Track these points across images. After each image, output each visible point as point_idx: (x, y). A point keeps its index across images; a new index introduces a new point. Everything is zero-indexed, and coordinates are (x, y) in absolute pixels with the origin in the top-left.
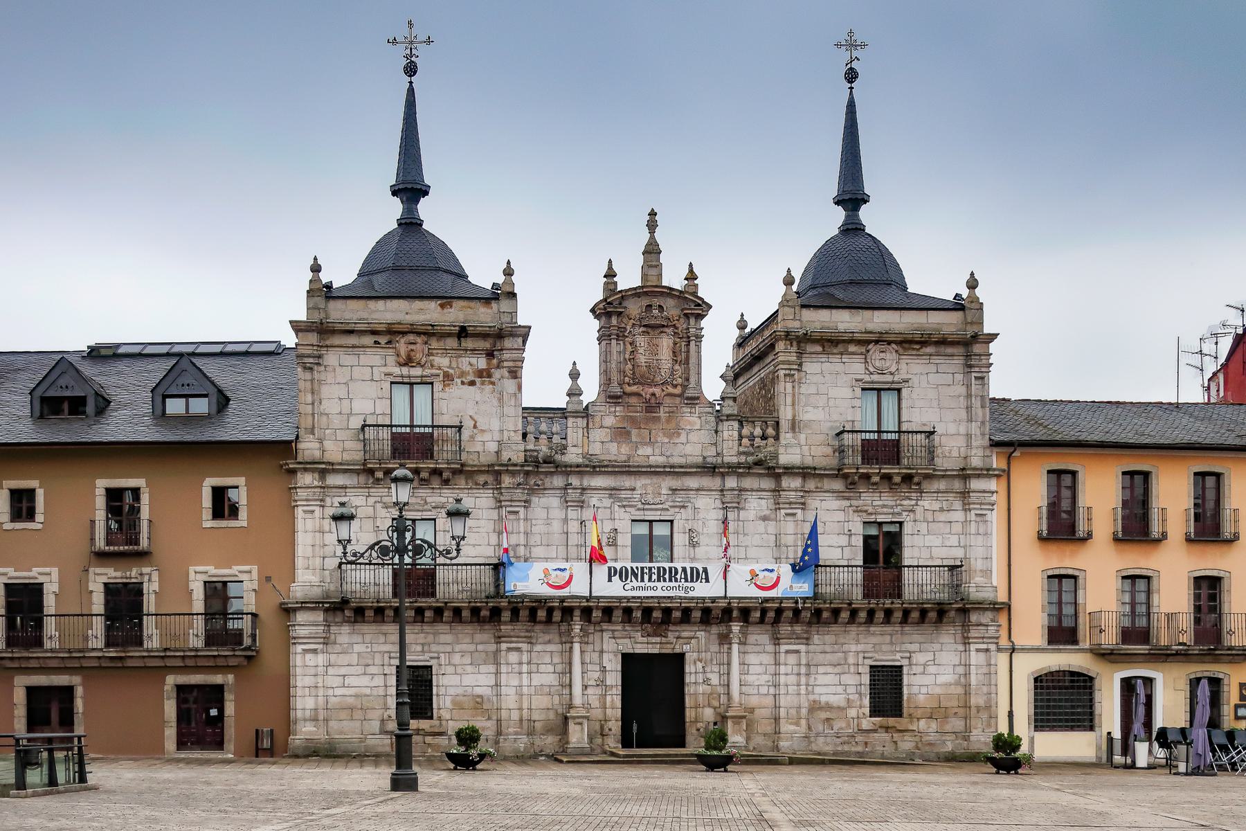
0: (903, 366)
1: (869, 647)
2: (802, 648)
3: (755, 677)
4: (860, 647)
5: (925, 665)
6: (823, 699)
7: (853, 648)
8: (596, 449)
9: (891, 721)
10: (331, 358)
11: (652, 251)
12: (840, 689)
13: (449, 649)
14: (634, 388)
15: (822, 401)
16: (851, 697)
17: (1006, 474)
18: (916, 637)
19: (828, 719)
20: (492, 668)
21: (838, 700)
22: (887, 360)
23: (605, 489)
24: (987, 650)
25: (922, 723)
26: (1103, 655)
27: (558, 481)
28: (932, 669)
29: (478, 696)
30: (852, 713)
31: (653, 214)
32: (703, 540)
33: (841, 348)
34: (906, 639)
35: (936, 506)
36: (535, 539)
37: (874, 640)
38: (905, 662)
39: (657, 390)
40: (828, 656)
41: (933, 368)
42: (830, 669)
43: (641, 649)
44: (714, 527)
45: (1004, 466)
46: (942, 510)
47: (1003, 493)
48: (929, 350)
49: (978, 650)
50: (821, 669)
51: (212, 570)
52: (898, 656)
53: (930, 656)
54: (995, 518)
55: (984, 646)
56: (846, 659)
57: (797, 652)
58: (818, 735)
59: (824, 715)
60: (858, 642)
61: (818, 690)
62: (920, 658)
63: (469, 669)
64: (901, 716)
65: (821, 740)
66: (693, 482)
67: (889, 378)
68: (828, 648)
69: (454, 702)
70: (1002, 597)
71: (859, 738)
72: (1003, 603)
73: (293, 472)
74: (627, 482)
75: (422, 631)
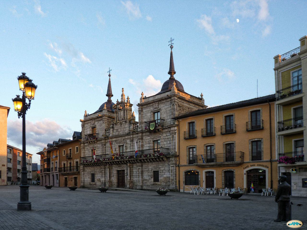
0: (160, 106)
1: (153, 167)
2: (141, 168)
3: (134, 174)
4: (151, 167)
5: (163, 170)
6: (145, 178)
7: (150, 167)
8: (114, 134)
9: (157, 183)
10: (85, 126)
11: (122, 95)
12: (148, 176)
13: (96, 170)
14: (118, 122)
15: (146, 117)
16: (150, 178)
17: (178, 126)
18: (161, 164)
19: (146, 183)
20: (100, 174)
21: (148, 178)
22: (156, 105)
23: (115, 141)
24: (173, 166)
25: (162, 183)
26: (199, 166)
27: (109, 140)
28: (164, 171)
29: (100, 178)
30: (150, 181)
31: (123, 89)
32: (128, 148)
33: (149, 105)
34: (160, 165)
35: (165, 135)
36: (106, 151)
37: (154, 165)
38: (159, 170)
39: (121, 121)
40: (146, 169)
41: (165, 105)
42: (146, 172)
43: (119, 169)
44: (129, 145)
45: (178, 124)
46: (166, 136)
47: (178, 130)
48: (164, 101)
49: (172, 167)
50: (145, 172)
51: (76, 160)
52: (157, 169)
53: (163, 168)
54: (176, 136)
55: (172, 166)
56: (149, 170)
57: (140, 169)
58: (144, 186)
59: (145, 181)
60: (151, 166)
61: (144, 176)
62: (162, 169)
63: (99, 174)
64: (159, 182)
65: (144, 186)
66: (126, 137)
67: (157, 109)
68: (146, 168)
69: (97, 180)
70: (178, 154)
71: (151, 186)
72: (178, 155)
73: (81, 144)
74: (118, 139)
75: (94, 168)
